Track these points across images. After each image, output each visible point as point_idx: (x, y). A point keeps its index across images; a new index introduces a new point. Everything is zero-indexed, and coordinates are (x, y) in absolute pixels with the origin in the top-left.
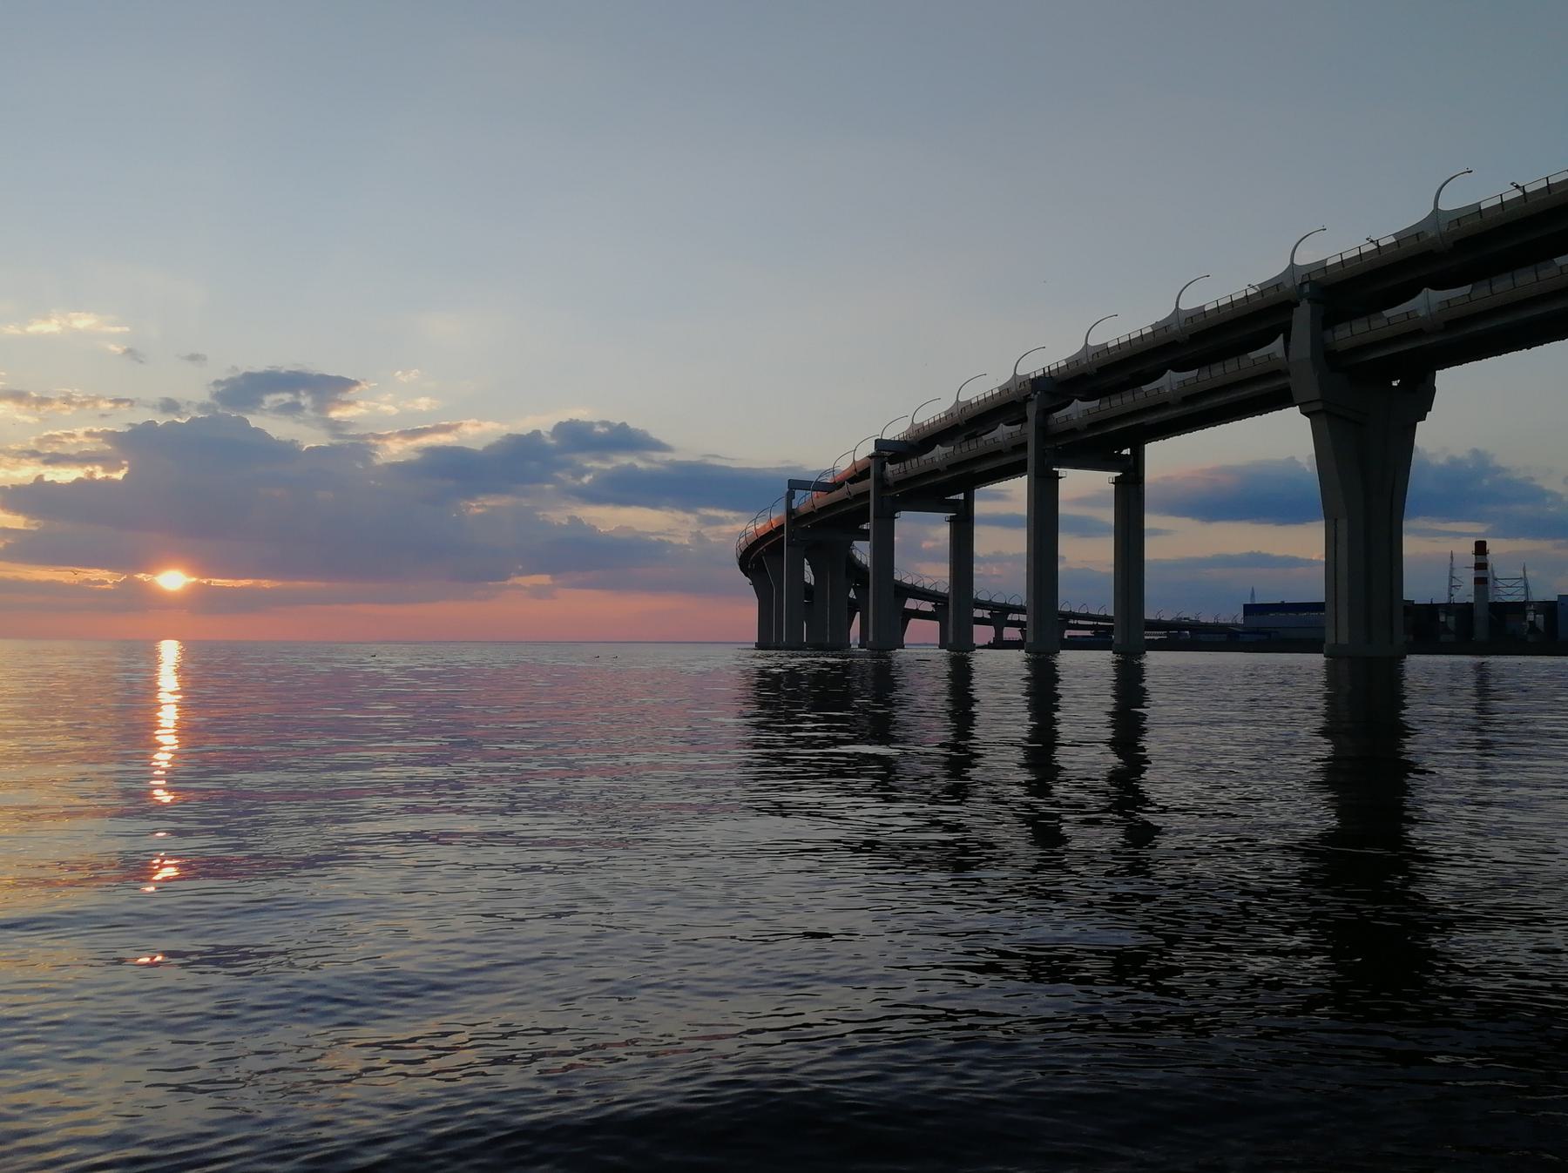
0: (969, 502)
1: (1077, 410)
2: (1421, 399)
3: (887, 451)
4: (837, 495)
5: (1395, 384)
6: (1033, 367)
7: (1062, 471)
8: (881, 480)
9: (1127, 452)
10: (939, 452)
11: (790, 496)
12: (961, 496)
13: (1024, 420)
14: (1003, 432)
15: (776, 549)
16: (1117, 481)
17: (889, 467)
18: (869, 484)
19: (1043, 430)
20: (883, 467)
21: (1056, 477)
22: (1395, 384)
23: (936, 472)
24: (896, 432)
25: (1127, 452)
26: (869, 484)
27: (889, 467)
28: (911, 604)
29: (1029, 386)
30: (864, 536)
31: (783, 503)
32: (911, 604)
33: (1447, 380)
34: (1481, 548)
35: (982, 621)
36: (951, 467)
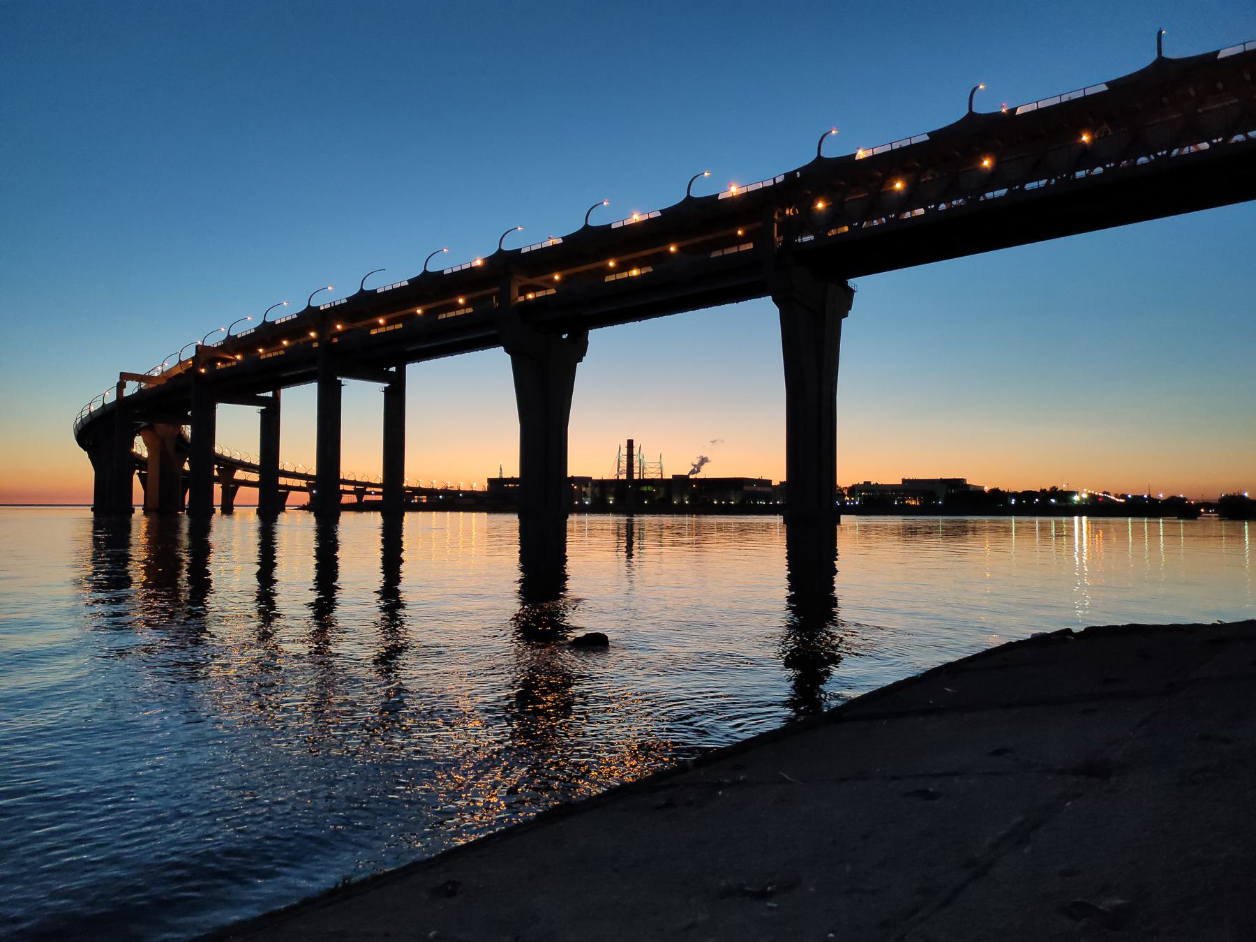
2: (579, 349)
3: (204, 354)
5: (564, 336)
7: (344, 380)
11: (121, 386)
12: (270, 394)
21: (339, 385)
22: (564, 336)
33: (594, 335)
34: (630, 443)
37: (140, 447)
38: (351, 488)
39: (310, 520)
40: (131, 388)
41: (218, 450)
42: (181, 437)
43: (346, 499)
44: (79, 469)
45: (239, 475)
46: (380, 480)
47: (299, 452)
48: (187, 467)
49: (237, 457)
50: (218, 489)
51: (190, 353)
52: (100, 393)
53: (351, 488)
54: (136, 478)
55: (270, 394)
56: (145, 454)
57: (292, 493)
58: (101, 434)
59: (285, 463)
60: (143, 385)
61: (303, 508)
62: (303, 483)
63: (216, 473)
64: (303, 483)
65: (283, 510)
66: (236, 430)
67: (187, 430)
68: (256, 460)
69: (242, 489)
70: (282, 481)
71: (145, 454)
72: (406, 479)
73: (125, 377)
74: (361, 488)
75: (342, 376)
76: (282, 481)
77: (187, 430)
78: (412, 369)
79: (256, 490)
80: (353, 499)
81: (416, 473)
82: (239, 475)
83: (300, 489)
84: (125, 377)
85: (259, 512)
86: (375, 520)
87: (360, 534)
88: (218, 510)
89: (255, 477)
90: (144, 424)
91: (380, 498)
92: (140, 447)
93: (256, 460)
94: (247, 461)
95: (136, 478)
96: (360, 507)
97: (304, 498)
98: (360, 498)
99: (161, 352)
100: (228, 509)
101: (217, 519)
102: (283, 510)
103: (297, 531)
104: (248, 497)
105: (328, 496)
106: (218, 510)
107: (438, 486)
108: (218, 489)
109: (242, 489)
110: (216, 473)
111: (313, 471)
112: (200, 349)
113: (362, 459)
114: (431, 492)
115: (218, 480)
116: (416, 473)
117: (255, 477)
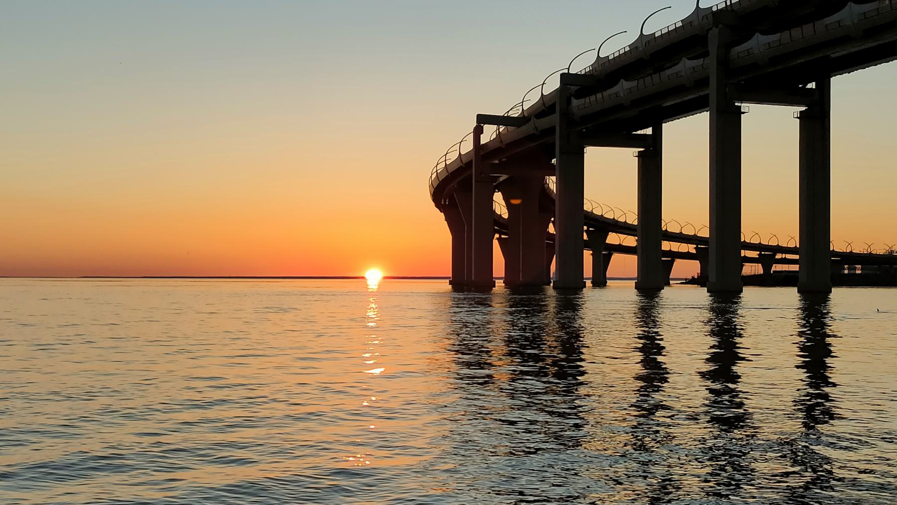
0: (658, 133)
1: (759, 44)
4: (526, 129)
6: (659, 25)
7: (744, 106)
8: (566, 115)
9: (812, 85)
10: (624, 86)
11: (478, 131)
12: (649, 131)
13: (706, 54)
14: (686, 66)
15: (466, 185)
16: (802, 116)
17: (575, 102)
18: (554, 119)
19: (724, 63)
20: (569, 102)
21: (739, 112)
23: (619, 108)
24: (582, 66)
25: (812, 85)
26: (554, 119)
27: (575, 102)
28: (613, 238)
29: (711, 18)
30: (551, 171)
31: (471, 138)
32: (613, 238)
35: (687, 256)
36: (636, 103)
37: (499, 205)
38: (754, 254)
39: (701, 296)
40: (489, 133)
41: (587, 207)
42: (545, 190)
43: (748, 269)
44: (435, 234)
46: (795, 243)
47: (687, 205)
48: (551, 229)
49: (610, 216)
50: (588, 256)
51: (554, 84)
52: (453, 141)
53: (754, 254)
54: (496, 243)
55: (649, 131)
56: (506, 216)
57: (678, 263)
58: (456, 191)
59: (671, 220)
60: (502, 128)
61: (692, 281)
62: (691, 248)
63: (585, 237)
64: (691, 248)
65: (668, 284)
66: (608, 178)
67: (552, 182)
68: (632, 219)
69: (616, 257)
70: (666, 246)
71: (506, 216)
72: (832, 237)
73: (483, 120)
74: (768, 253)
75: (742, 101)
76: (666, 246)
77: (552, 182)
78: (842, 86)
79: (633, 259)
80: (757, 269)
81: (847, 233)
83: (687, 256)
84: (483, 120)
85: (637, 287)
86: (790, 297)
87: (770, 317)
88: (589, 283)
89: (630, 241)
90: (503, 177)
91: (795, 268)
92: (499, 205)
93: (632, 219)
94: (622, 220)
95: (496, 243)
96: (767, 280)
97: (693, 268)
98: (767, 268)
99: (520, 85)
100: (600, 281)
102: (668, 284)
103: (685, 307)
104: (624, 265)
105: (725, 262)
106: (589, 283)
107: (880, 249)
108: (588, 256)
109: (616, 257)
110: (585, 237)
111: (705, 233)
112: (566, 78)
113: (770, 211)
114: (867, 259)
115: (587, 245)
116: (847, 233)
117: (630, 241)
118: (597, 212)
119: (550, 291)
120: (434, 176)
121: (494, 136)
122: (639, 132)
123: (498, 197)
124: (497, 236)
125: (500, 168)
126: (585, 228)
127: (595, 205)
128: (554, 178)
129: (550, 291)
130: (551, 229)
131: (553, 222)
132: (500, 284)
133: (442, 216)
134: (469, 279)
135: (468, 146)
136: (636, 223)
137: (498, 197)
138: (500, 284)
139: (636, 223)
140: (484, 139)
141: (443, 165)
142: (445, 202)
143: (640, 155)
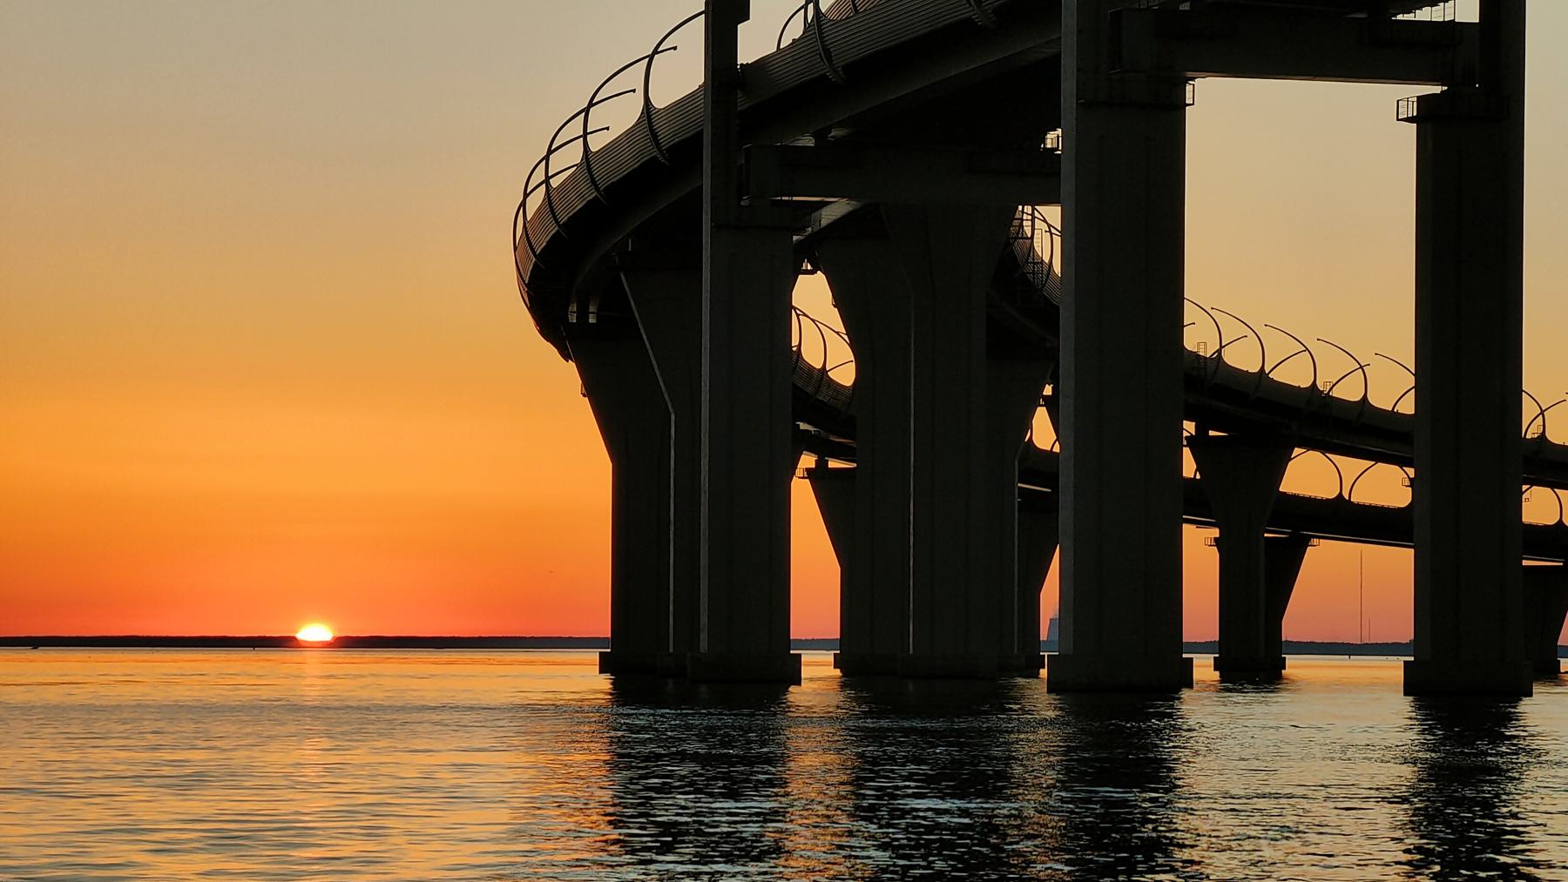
31: (694, 40)
41: (1198, 337)
42: (1013, 261)
45: (1310, 474)
48: (1043, 432)
49: (1294, 375)
50: (1199, 548)
54: (802, 494)
56: (844, 373)
58: (624, 262)
63: (1189, 468)
67: (1045, 231)
68: (1393, 388)
69: (1326, 560)
71: (844, 373)
77: (1045, 231)
79: (1394, 566)
82: (1310, 474)
85: (1412, 686)
88: (1204, 668)
89: (1386, 485)
90: (835, 209)
93: (1393, 388)
94: (1349, 392)
95: (802, 494)
100: (1254, 659)
101: (1208, 714)
104: (1357, 587)
106: (1204, 668)
108: (1199, 548)
109: (1326, 560)
110: (1189, 468)
115: (1197, 502)
117: (1386, 485)
118: (1243, 359)
119: (1038, 696)
120: (536, 201)
121: (796, 30)
122: (1424, 14)
123: (812, 294)
124: (808, 461)
125: (825, 170)
126: (1189, 427)
127: (1231, 330)
128: (1053, 213)
129: (1038, 696)
130: (1043, 432)
131: (1052, 405)
132: (819, 671)
133: (568, 374)
134: (681, 648)
135: (682, 75)
136: (1408, 407)
137: (812, 294)
138: (819, 671)
139: (1408, 407)
140: (755, 42)
141: (574, 154)
142: (583, 314)
143: (1427, 116)
